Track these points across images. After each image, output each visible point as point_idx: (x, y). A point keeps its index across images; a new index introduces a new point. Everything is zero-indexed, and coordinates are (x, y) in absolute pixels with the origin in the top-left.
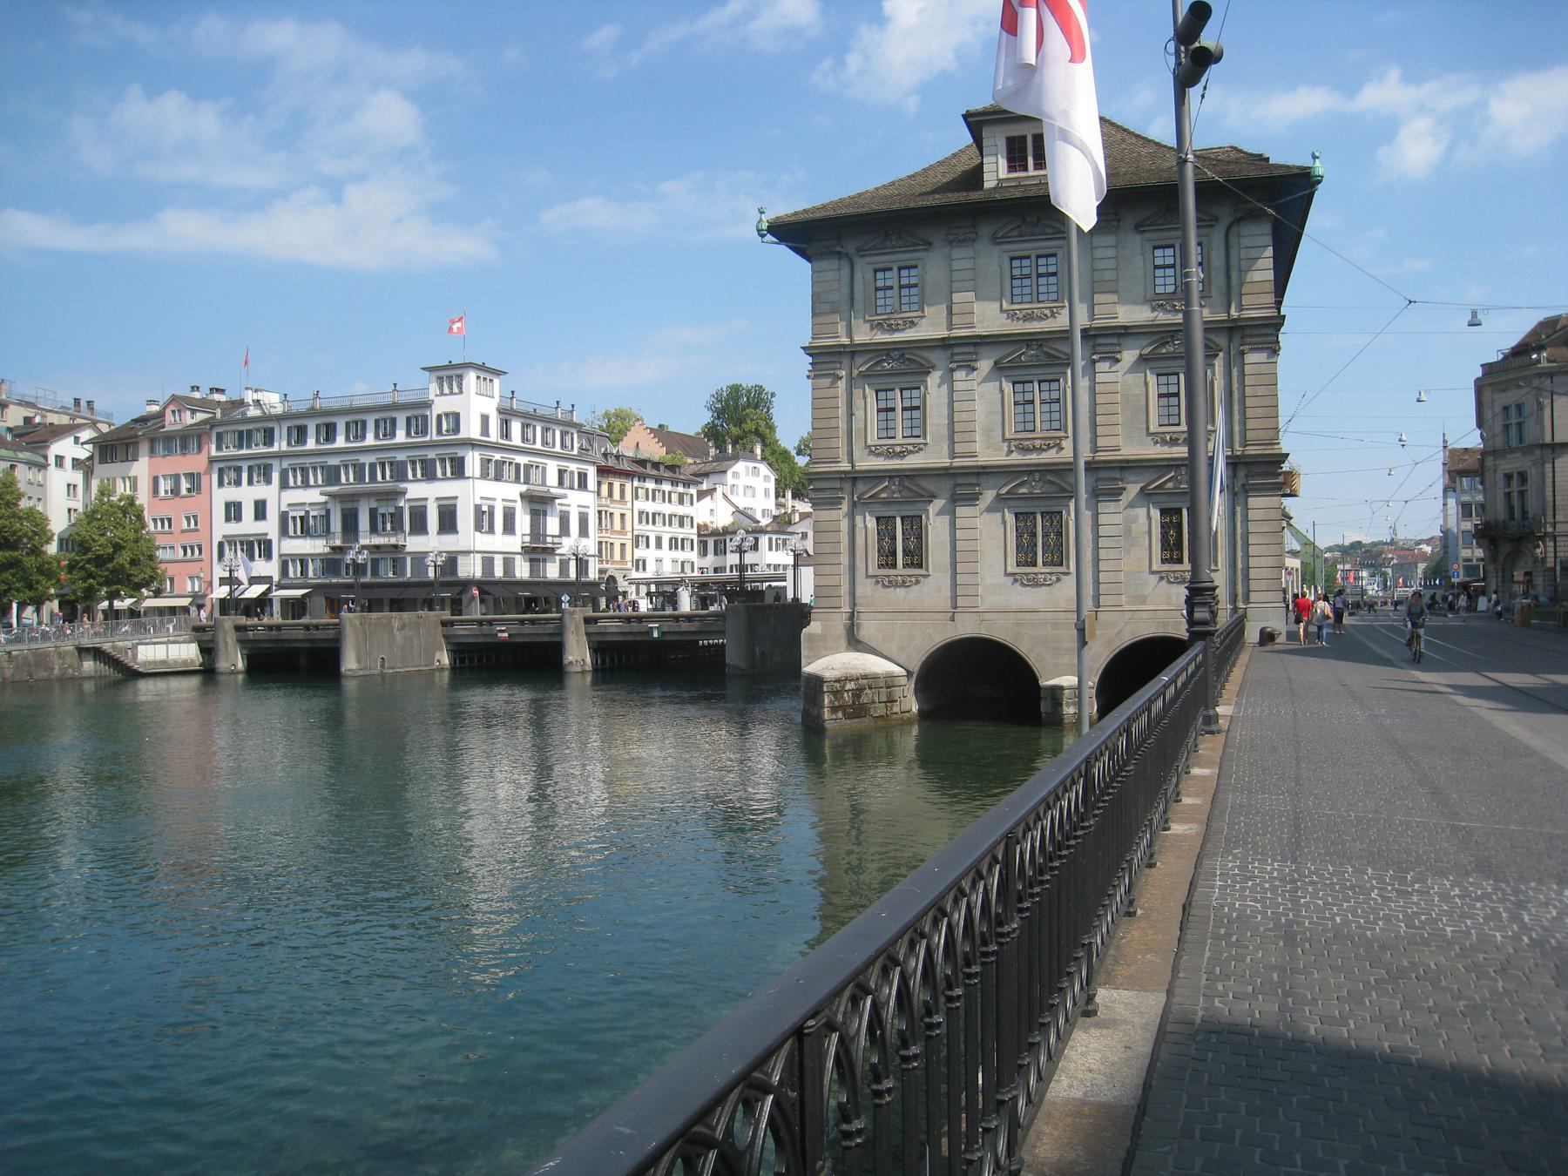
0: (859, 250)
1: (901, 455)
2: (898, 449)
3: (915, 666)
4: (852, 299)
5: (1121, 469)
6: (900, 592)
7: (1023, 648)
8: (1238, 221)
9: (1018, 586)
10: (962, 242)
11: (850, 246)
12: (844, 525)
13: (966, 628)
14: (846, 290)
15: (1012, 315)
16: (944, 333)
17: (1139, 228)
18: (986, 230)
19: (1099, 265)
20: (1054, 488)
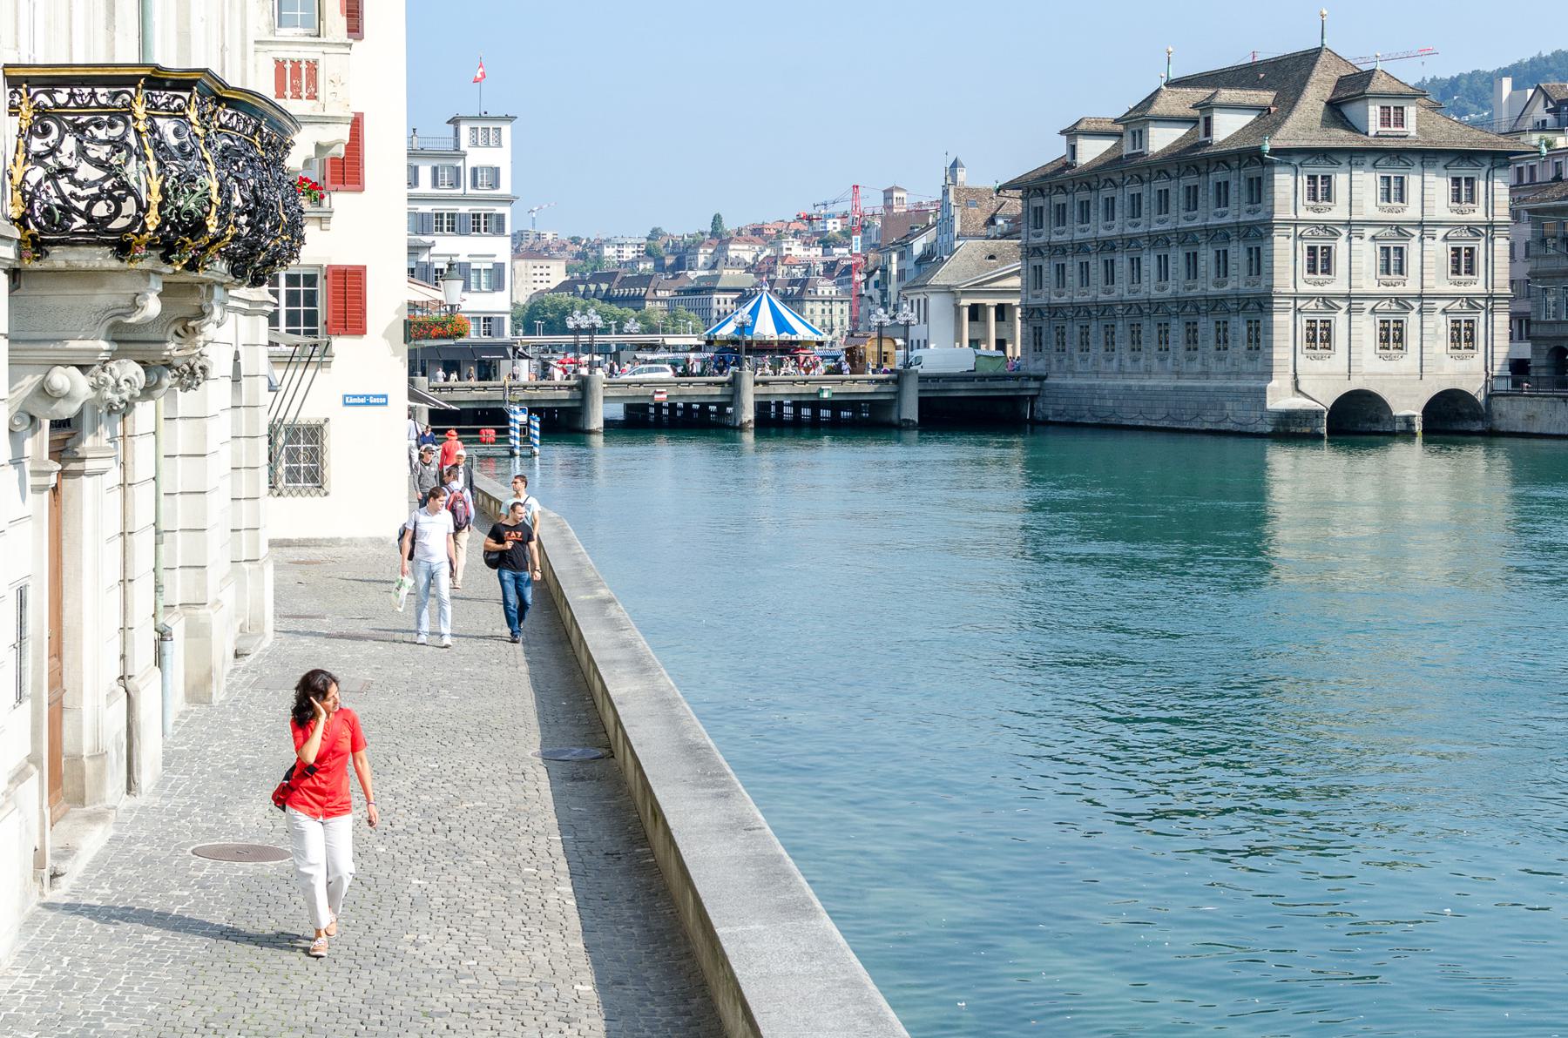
10: (1359, 165)
11: (1296, 161)
13: (1356, 384)
15: (1381, 209)
18: (1369, 160)
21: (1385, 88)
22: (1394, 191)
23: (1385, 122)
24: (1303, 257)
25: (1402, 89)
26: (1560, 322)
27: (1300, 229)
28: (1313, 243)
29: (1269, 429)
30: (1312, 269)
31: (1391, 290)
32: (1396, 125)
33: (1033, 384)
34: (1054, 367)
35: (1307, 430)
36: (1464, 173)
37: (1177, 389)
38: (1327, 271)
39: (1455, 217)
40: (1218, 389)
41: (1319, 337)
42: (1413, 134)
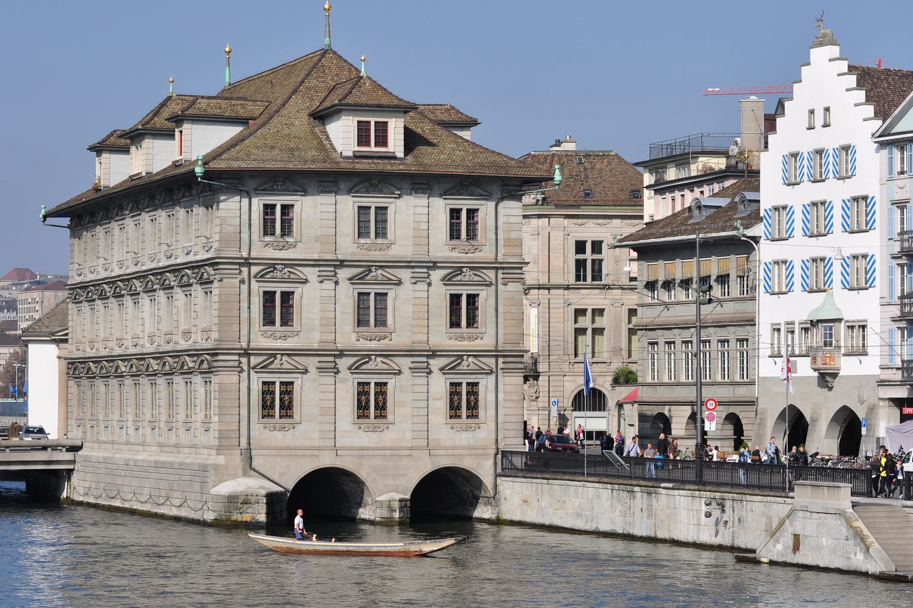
0: (256, 190)
1: (285, 338)
2: (278, 334)
3: (290, 486)
4: (250, 225)
5: (428, 356)
6: (279, 435)
7: (362, 474)
8: (502, 199)
9: (361, 432)
12: (244, 386)
13: (327, 461)
14: (245, 217)
16: (316, 257)
17: (444, 194)
19: (419, 218)
20: (385, 366)
21: (364, 100)
22: (372, 224)
23: (363, 139)
24: (257, 303)
25: (385, 101)
26: (733, 384)
27: (255, 270)
28: (270, 287)
29: (210, 516)
30: (269, 320)
31: (373, 345)
32: (376, 146)
33: (69, 456)
34: (89, 437)
35: (247, 517)
36: (464, 204)
37: (158, 465)
38: (287, 320)
39: (456, 255)
40: (182, 466)
41: (278, 403)
42: (400, 154)
